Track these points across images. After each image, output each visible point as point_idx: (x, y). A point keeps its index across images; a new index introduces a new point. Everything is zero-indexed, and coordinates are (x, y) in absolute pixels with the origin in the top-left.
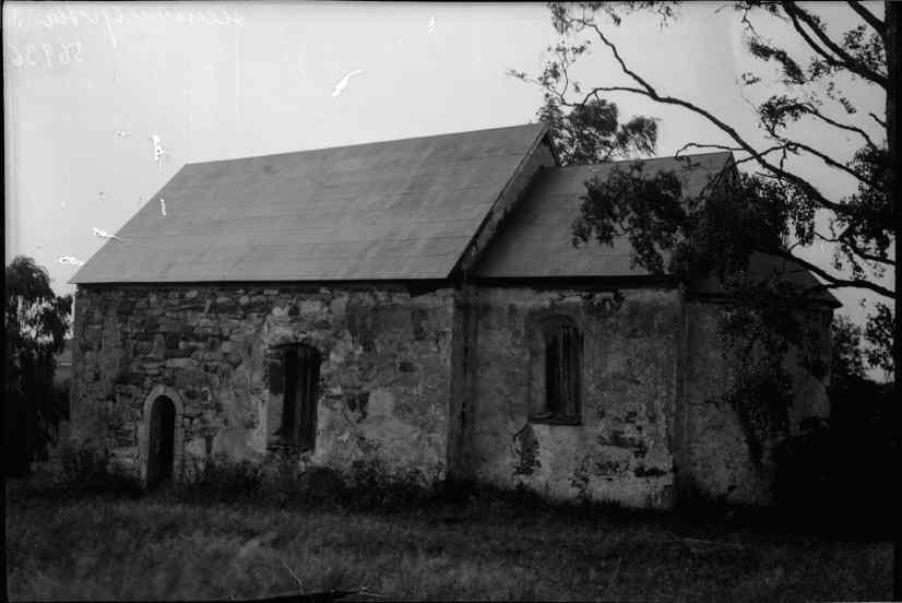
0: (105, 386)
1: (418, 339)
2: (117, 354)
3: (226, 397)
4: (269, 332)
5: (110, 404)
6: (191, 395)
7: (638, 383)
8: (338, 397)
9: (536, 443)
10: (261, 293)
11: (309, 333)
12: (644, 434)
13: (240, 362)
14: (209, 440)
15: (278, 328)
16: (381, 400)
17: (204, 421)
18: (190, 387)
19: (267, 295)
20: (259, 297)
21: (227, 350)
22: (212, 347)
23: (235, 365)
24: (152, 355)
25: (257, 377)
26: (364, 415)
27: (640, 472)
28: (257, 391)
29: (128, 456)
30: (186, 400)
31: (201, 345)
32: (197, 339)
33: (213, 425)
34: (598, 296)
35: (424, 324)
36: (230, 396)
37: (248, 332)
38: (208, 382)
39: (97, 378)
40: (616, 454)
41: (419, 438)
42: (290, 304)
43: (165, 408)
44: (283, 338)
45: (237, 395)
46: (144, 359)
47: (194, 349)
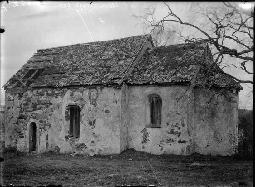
0: (15, 119)
2: (19, 109)
5: (17, 125)
6: (41, 122)
7: (179, 114)
10: (61, 90)
16: (99, 122)
18: (41, 119)
21: (51, 108)
22: (47, 107)
24: (29, 110)
26: (94, 127)
27: (180, 142)
29: (23, 141)
31: (44, 106)
32: (43, 104)
39: (12, 117)
40: (172, 136)
43: (34, 126)
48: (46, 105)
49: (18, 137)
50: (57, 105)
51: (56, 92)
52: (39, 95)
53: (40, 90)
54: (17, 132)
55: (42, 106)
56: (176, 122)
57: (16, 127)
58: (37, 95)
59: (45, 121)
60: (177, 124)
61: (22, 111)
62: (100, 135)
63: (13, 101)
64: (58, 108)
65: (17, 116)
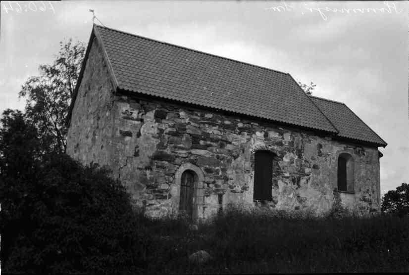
1: (319, 155)
2: (155, 142)
3: (230, 173)
4: (254, 143)
5: (148, 172)
6: (208, 171)
9: (341, 200)
11: (272, 147)
12: (371, 197)
13: (238, 156)
14: (220, 197)
15: (258, 141)
17: (216, 186)
18: (207, 166)
19: (252, 125)
21: (230, 149)
22: (222, 146)
23: (235, 158)
24: (182, 145)
25: (248, 165)
26: (299, 186)
28: (249, 172)
30: (205, 173)
31: (214, 144)
32: (212, 140)
34: (358, 148)
35: (321, 150)
36: (232, 173)
37: (242, 142)
38: (218, 164)
39: (136, 154)
40: (365, 204)
41: (321, 197)
42: (264, 131)
45: (237, 173)
46: (175, 147)
47: (210, 146)
48: (219, 142)
49: (152, 196)
50: (241, 147)
51: (240, 125)
52: (207, 123)
53: (209, 116)
54: (148, 187)
55: (212, 143)
56: (367, 188)
57: (146, 175)
58: (201, 123)
59: (218, 169)
60: (368, 190)
61: (165, 145)
62: (306, 199)
63: (139, 122)
64: (243, 152)
65: (151, 153)
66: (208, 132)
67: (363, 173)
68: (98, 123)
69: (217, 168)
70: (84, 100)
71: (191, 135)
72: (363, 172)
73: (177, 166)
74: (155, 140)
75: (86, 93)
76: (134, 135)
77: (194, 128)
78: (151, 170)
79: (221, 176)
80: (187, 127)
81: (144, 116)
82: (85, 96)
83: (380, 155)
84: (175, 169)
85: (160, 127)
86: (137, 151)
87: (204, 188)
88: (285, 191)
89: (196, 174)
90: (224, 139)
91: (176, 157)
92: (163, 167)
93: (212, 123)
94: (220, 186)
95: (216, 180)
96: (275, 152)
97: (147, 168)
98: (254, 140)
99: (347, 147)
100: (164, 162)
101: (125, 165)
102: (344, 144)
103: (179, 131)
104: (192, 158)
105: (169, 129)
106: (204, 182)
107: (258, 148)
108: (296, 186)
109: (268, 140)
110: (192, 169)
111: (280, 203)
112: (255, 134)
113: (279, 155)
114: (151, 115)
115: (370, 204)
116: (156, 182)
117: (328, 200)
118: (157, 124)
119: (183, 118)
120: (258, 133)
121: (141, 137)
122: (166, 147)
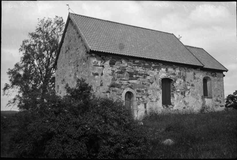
0: (106, 87)
1: (194, 79)
2: (111, 77)
3: (150, 92)
5: (108, 94)
6: (138, 91)
8: (179, 92)
9: (205, 102)
10: (158, 64)
11: (170, 76)
14: (145, 104)
15: (163, 73)
17: (143, 99)
18: (138, 89)
20: (157, 65)
21: (149, 79)
22: (145, 77)
23: (152, 83)
24: (124, 79)
25: (158, 87)
26: (185, 96)
27: (221, 106)
30: (137, 93)
31: (141, 77)
32: (139, 75)
33: (146, 100)
34: (213, 73)
35: (195, 76)
37: (155, 74)
38: (143, 87)
39: (101, 85)
40: (217, 103)
44: (164, 76)
45: (153, 91)
46: (121, 80)
47: (138, 78)
48: (143, 75)
50: (154, 77)
51: (153, 65)
53: (137, 61)
55: (139, 76)
58: (134, 66)
60: (219, 95)
61: (116, 79)
63: (102, 67)
64: (156, 80)
65: (109, 84)
66: (137, 70)
67: (216, 87)
68: (77, 69)
69: (143, 89)
70: (66, 55)
71: (128, 73)
72: (216, 86)
73: (122, 90)
74: (111, 76)
75: (67, 51)
76: (100, 75)
77: (130, 69)
78: (110, 93)
79: (145, 93)
80: (126, 68)
81: (104, 64)
82: (66, 53)
83: (224, 76)
84: (122, 91)
85: (112, 70)
86: (102, 83)
87: (137, 100)
88: (178, 99)
89: (132, 93)
90: (146, 74)
91: (122, 85)
92: (115, 91)
93: (139, 65)
94: (145, 99)
95: (143, 96)
96: (172, 79)
97: (107, 92)
98: (161, 73)
99: (208, 73)
100: (116, 88)
101: (96, 91)
102: (205, 71)
103: (122, 71)
104: (130, 85)
105: (117, 70)
106: (137, 97)
107: (163, 77)
108: (183, 96)
109: (168, 72)
110: (130, 91)
111: (175, 106)
112: (161, 70)
113: (174, 80)
114: (108, 63)
115: (220, 103)
116: (112, 99)
117: (200, 102)
118: (111, 68)
119: (124, 64)
120: (163, 69)
121: (103, 76)
122: (116, 80)
